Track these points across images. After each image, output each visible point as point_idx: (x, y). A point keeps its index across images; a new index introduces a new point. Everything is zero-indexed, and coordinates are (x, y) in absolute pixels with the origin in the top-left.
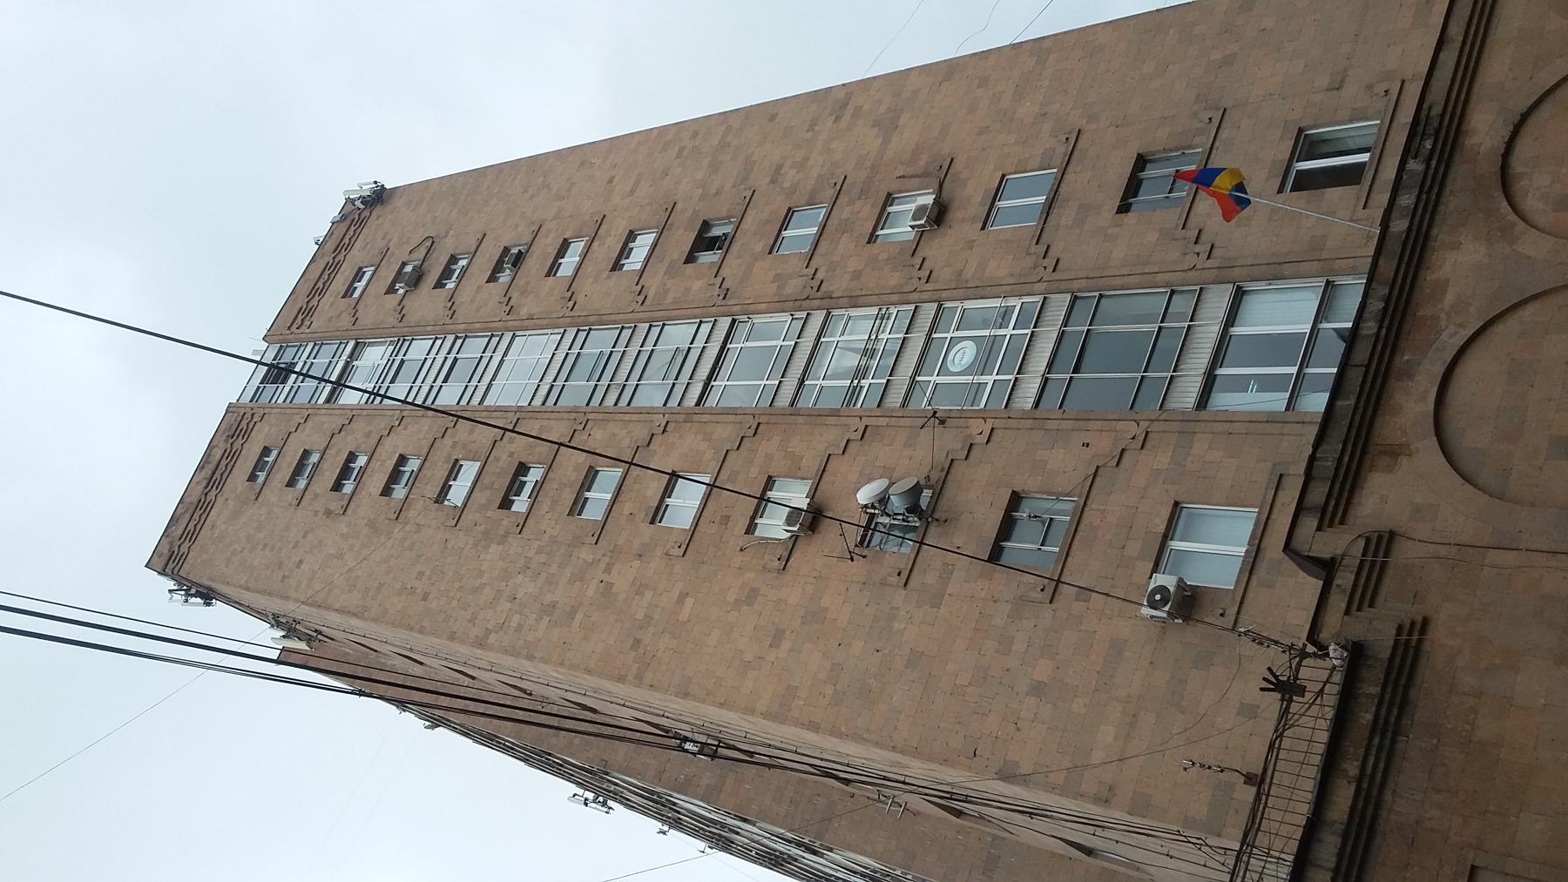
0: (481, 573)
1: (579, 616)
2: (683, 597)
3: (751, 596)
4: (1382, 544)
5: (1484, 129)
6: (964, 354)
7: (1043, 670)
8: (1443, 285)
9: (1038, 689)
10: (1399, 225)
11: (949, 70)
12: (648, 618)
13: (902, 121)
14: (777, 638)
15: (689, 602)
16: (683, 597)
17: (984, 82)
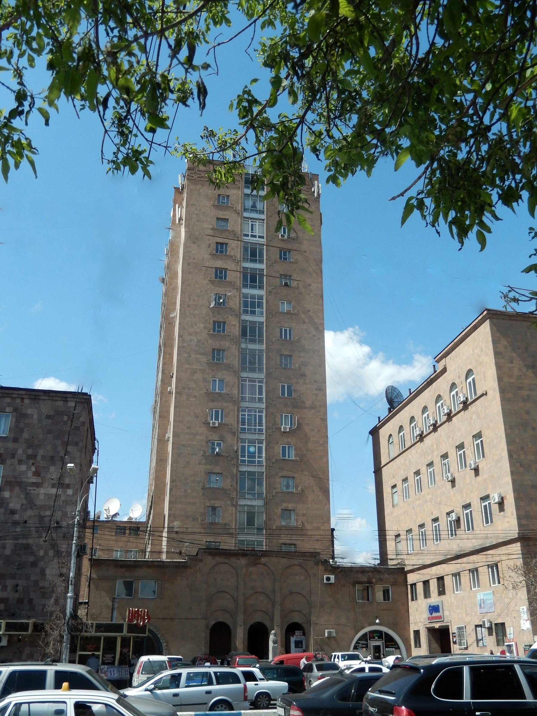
0: (196, 325)
1: (188, 366)
2: (195, 397)
3: (197, 417)
4: (201, 561)
5: (263, 560)
6: (252, 449)
7: (189, 491)
8: (239, 560)
9: (186, 491)
10: (248, 552)
11: (324, 420)
12: (189, 389)
13: (313, 411)
14: (189, 428)
15: (194, 399)
16: (195, 397)
17: (319, 431)
